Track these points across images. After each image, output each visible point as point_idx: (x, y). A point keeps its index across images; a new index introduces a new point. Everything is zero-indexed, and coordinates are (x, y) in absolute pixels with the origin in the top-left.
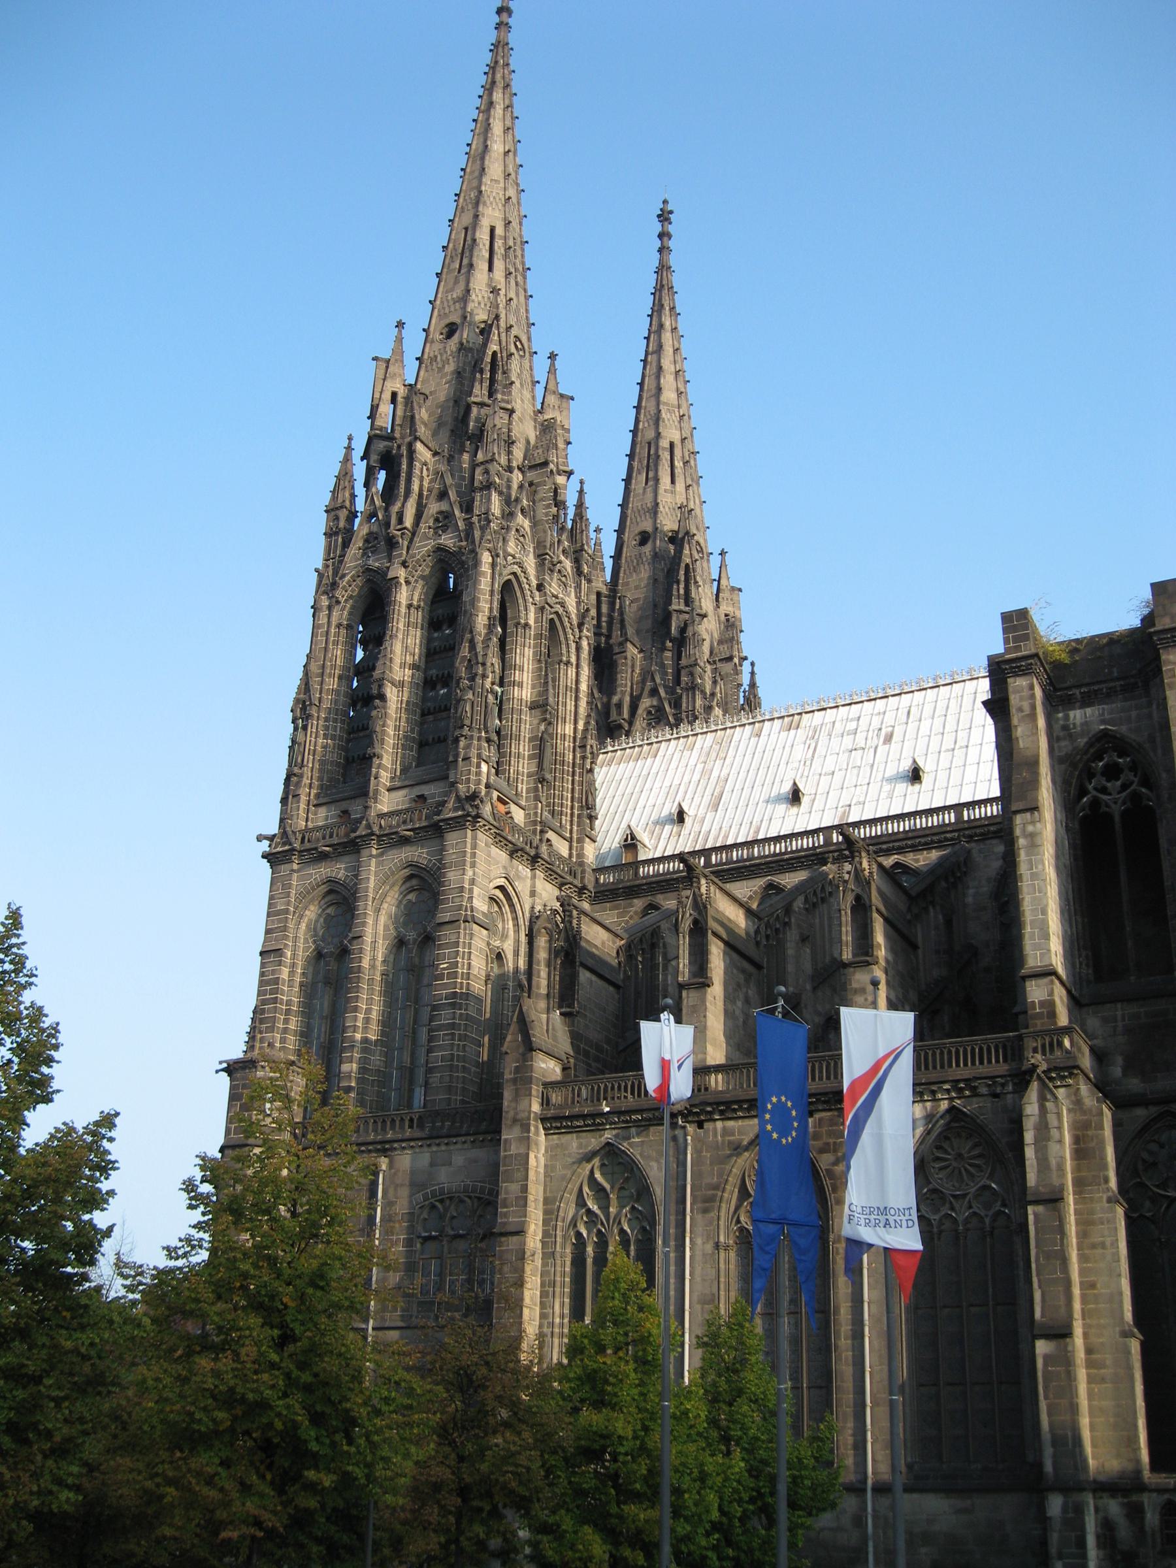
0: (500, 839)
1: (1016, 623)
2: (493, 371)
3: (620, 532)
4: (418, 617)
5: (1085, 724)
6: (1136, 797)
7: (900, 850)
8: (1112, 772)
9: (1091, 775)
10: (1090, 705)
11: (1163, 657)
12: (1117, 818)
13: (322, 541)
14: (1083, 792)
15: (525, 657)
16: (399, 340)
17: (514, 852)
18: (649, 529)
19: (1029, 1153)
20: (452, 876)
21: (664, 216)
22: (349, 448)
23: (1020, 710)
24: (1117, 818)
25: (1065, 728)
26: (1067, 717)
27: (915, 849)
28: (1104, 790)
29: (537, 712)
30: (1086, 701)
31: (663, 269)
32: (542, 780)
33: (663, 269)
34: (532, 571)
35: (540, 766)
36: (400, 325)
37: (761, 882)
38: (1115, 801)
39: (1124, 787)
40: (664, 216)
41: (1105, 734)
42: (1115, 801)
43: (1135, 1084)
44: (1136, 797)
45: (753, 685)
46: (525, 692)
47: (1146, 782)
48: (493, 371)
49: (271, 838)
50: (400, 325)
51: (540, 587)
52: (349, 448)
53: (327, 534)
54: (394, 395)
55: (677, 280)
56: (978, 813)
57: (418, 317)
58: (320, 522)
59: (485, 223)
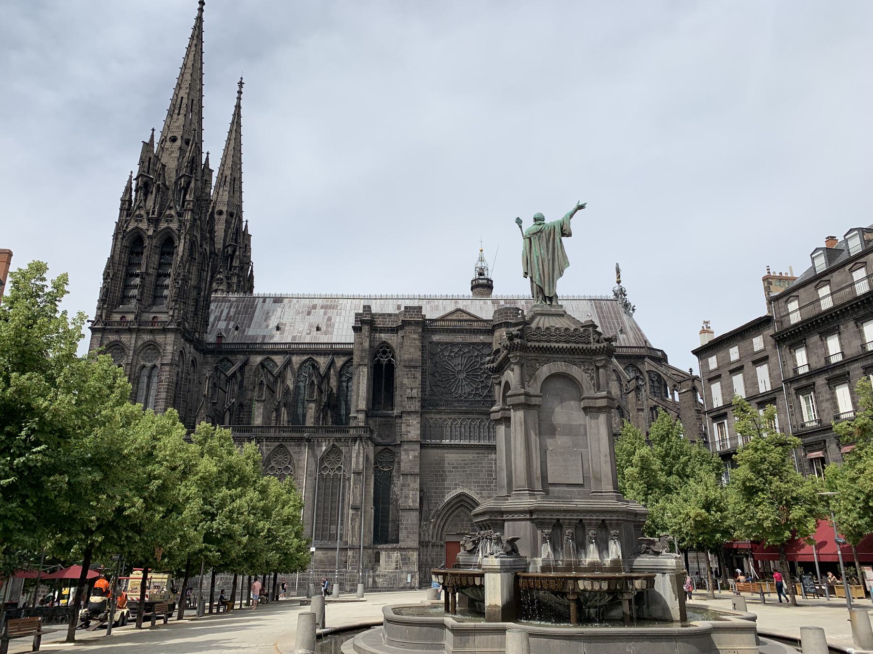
0: (183, 336)
1: (367, 308)
2: (193, 163)
4: (158, 250)
6: (390, 360)
7: (312, 354)
8: (384, 352)
13: (119, 211)
14: (376, 357)
16: (152, 136)
17: (187, 340)
18: (225, 209)
19: (354, 460)
20: (169, 348)
21: (241, 84)
22: (131, 177)
27: (317, 354)
29: (196, 290)
31: (238, 107)
32: (196, 314)
33: (238, 107)
35: (196, 308)
36: (153, 130)
37: (266, 357)
38: (384, 361)
40: (241, 84)
41: (384, 342)
42: (384, 361)
43: (379, 440)
45: (252, 271)
46: (193, 283)
47: (393, 357)
48: (193, 163)
49: (93, 322)
50: (153, 130)
51: (201, 246)
52: (131, 177)
53: (121, 210)
54: (150, 159)
55: (243, 112)
56: (338, 346)
57: (160, 127)
58: (119, 204)
59: (190, 97)
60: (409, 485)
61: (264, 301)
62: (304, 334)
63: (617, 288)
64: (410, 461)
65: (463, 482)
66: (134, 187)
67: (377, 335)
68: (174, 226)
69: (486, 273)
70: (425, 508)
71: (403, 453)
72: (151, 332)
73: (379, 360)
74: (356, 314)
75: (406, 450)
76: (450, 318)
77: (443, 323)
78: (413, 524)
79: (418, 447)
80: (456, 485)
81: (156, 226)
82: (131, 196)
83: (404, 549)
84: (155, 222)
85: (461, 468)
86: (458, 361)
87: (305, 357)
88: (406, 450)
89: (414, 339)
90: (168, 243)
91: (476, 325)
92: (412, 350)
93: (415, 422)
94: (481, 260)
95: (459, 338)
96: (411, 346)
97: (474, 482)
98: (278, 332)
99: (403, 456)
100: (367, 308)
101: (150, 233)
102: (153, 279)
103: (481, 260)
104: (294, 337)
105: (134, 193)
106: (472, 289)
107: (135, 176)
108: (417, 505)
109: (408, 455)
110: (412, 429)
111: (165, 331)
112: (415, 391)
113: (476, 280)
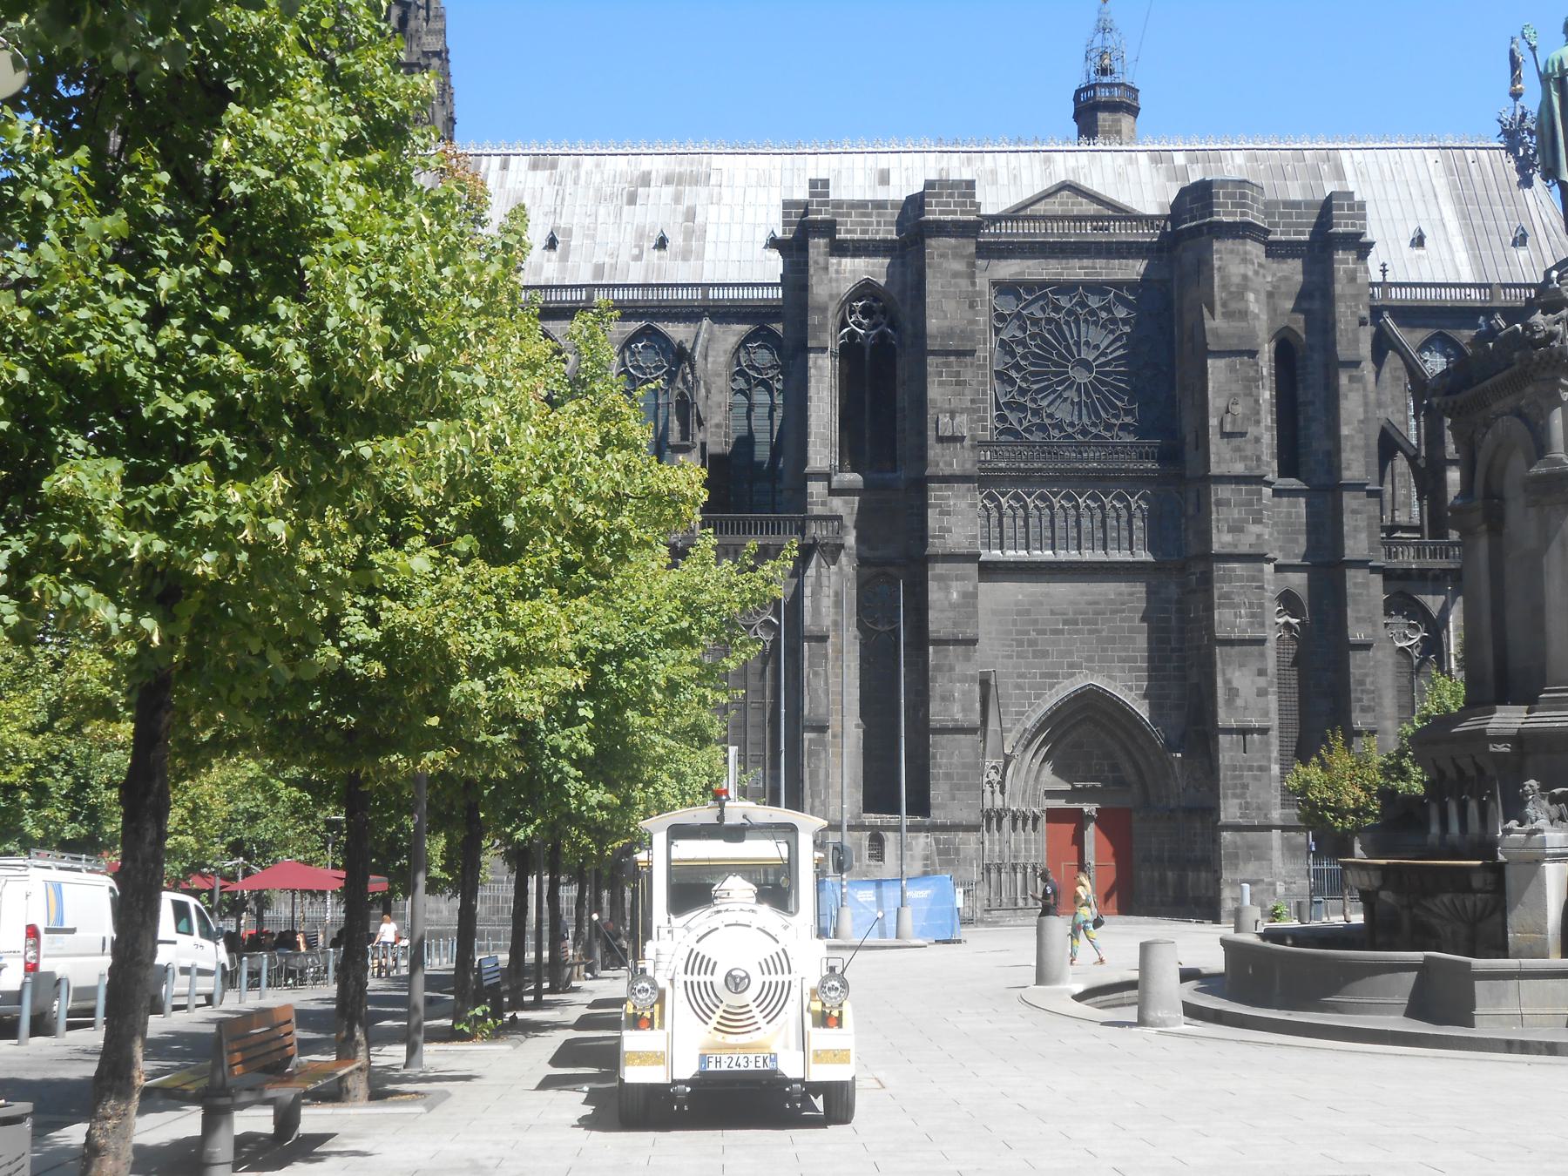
5: (853, 272)
9: (852, 312)
10: (860, 256)
11: (928, 241)
12: (868, 350)
14: (844, 324)
19: (807, 602)
23: (816, 262)
24: (868, 350)
25: (837, 272)
26: (839, 264)
28: (860, 325)
30: (854, 256)
39: (875, 326)
44: (882, 335)
60: (952, 669)
61: (505, 167)
62: (624, 258)
63: (1507, 116)
64: (953, 606)
65: (1090, 659)
67: (847, 262)
69: (1117, 67)
70: (993, 725)
71: (932, 586)
73: (852, 334)
74: (787, 205)
75: (941, 578)
76: (1040, 208)
77: (1027, 227)
78: (964, 766)
79: (972, 569)
80: (1071, 666)
83: (944, 828)
85: (1085, 622)
88: (941, 578)
89: (956, 275)
91: (1120, 233)
92: (950, 306)
93: (963, 504)
94: (1104, 29)
95: (1075, 270)
96: (945, 295)
97: (1122, 660)
98: (554, 255)
99: (935, 594)
100: (819, 186)
103: (1104, 29)
104: (599, 269)
106: (1076, 117)
108: (976, 718)
109: (947, 590)
110: (955, 520)
112: (962, 419)
113: (1092, 87)
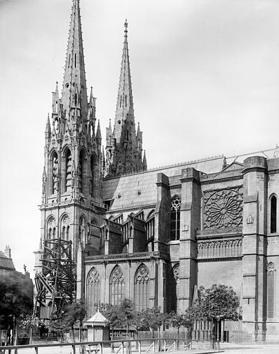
3: (116, 119)
8: (177, 202)
15: (87, 166)
34: (86, 146)
66: (51, 123)
68: (69, 142)
72: (64, 207)
81: (61, 145)
82: (50, 128)
84: (60, 141)
86: (222, 201)
87: (151, 210)
90: (68, 153)
101: (59, 150)
102: (63, 176)
105: (52, 127)
107: (51, 116)
111: (69, 206)
